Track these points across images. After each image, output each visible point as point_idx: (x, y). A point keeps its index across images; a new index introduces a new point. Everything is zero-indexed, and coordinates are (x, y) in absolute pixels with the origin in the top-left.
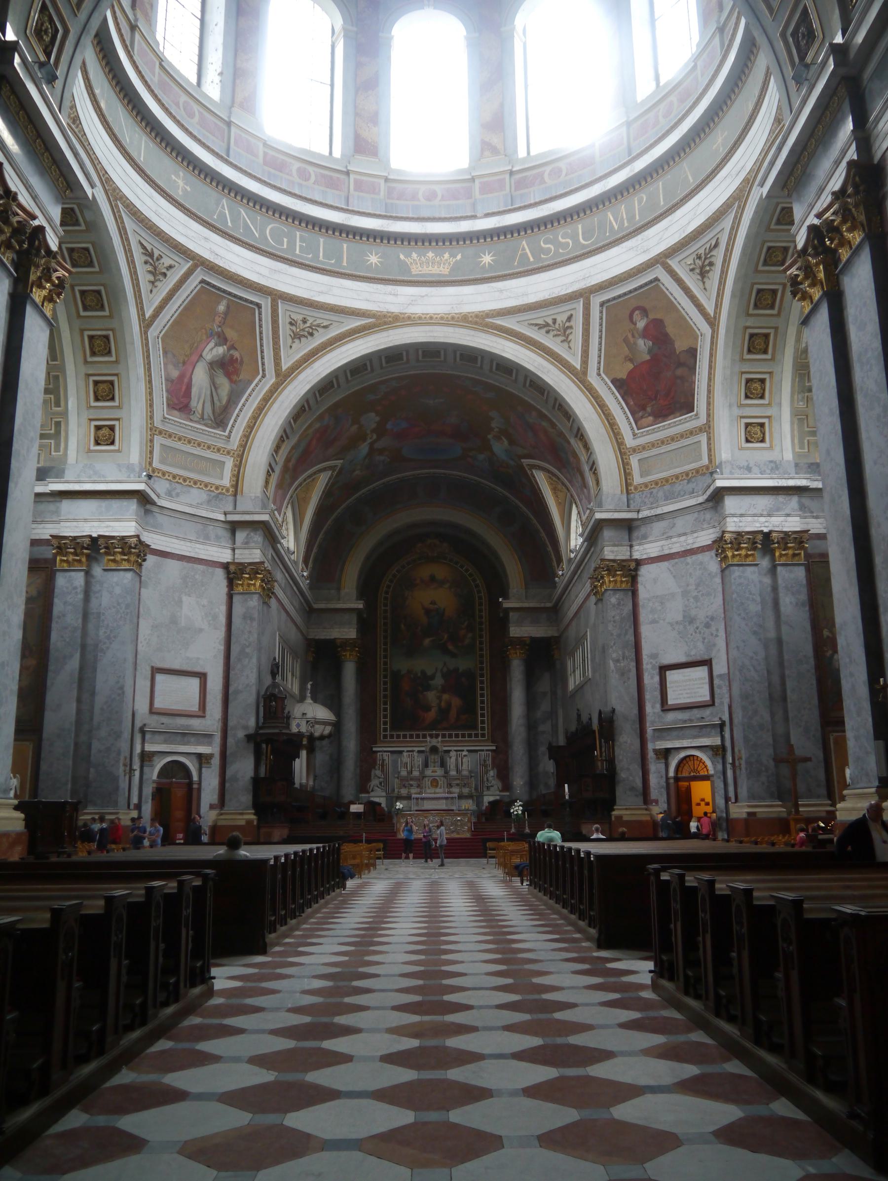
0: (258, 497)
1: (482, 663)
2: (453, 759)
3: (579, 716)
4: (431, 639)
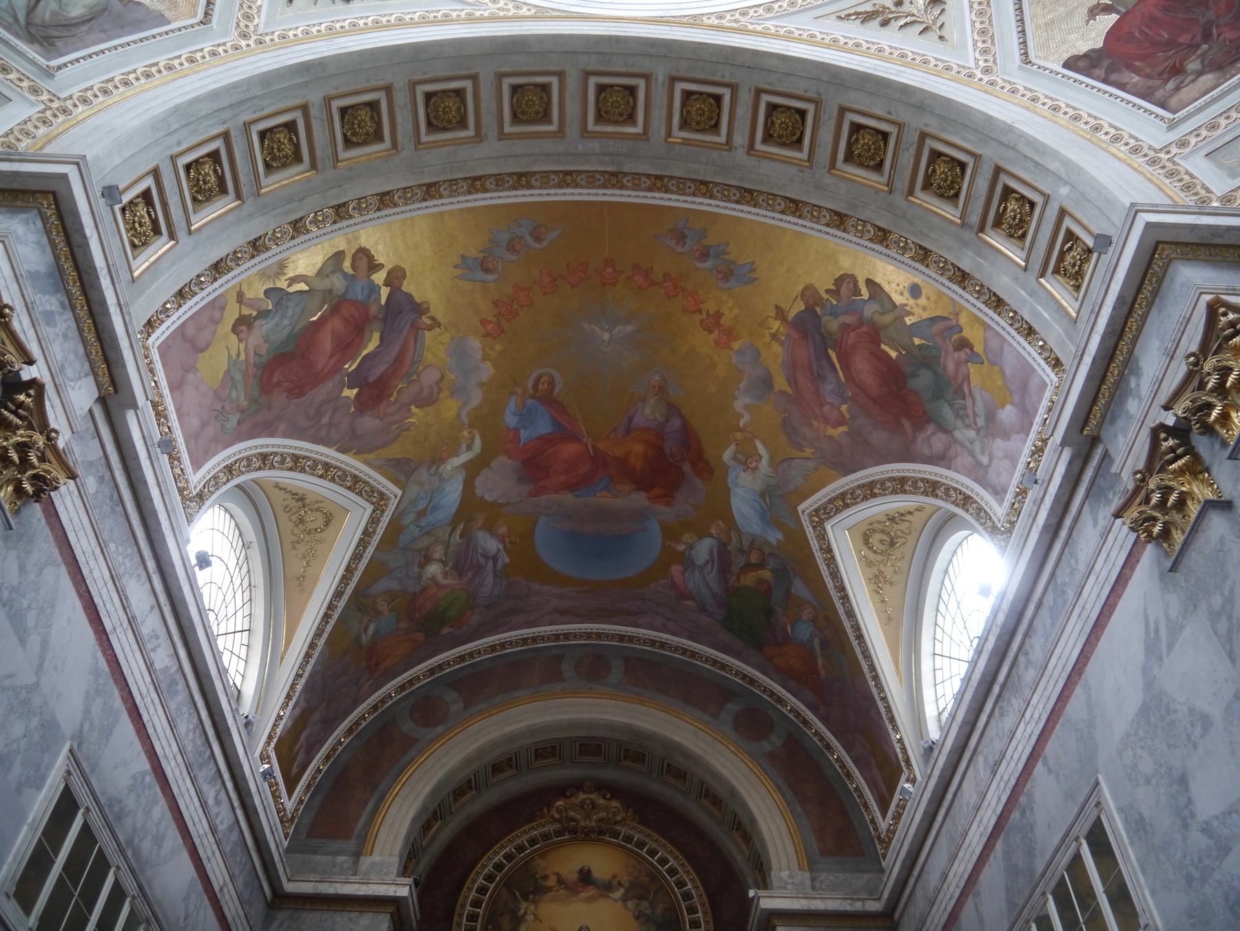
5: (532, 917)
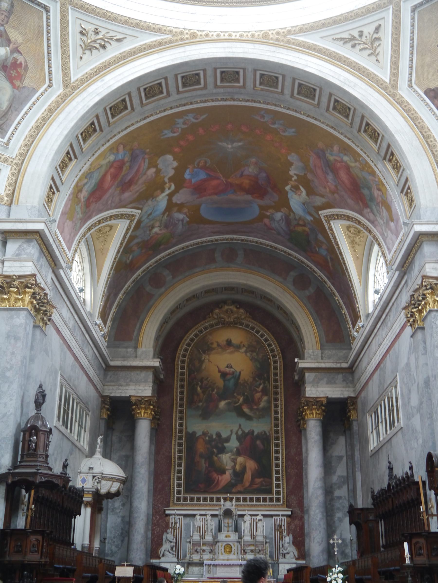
0: (35, 207)
1: (277, 425)
2: (248, 524)
3: (391, 469)
4: (227, 401)
5: (208, 361)
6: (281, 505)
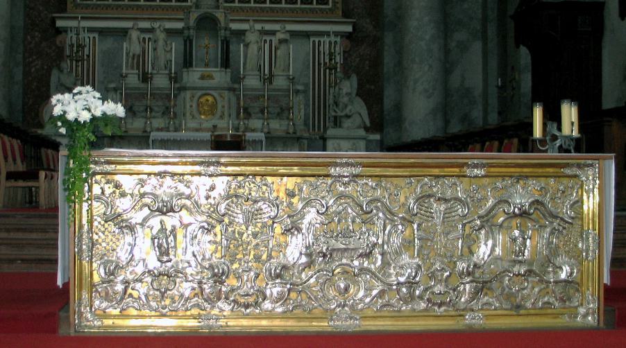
2: (253, 49)
6: (330, 9)
